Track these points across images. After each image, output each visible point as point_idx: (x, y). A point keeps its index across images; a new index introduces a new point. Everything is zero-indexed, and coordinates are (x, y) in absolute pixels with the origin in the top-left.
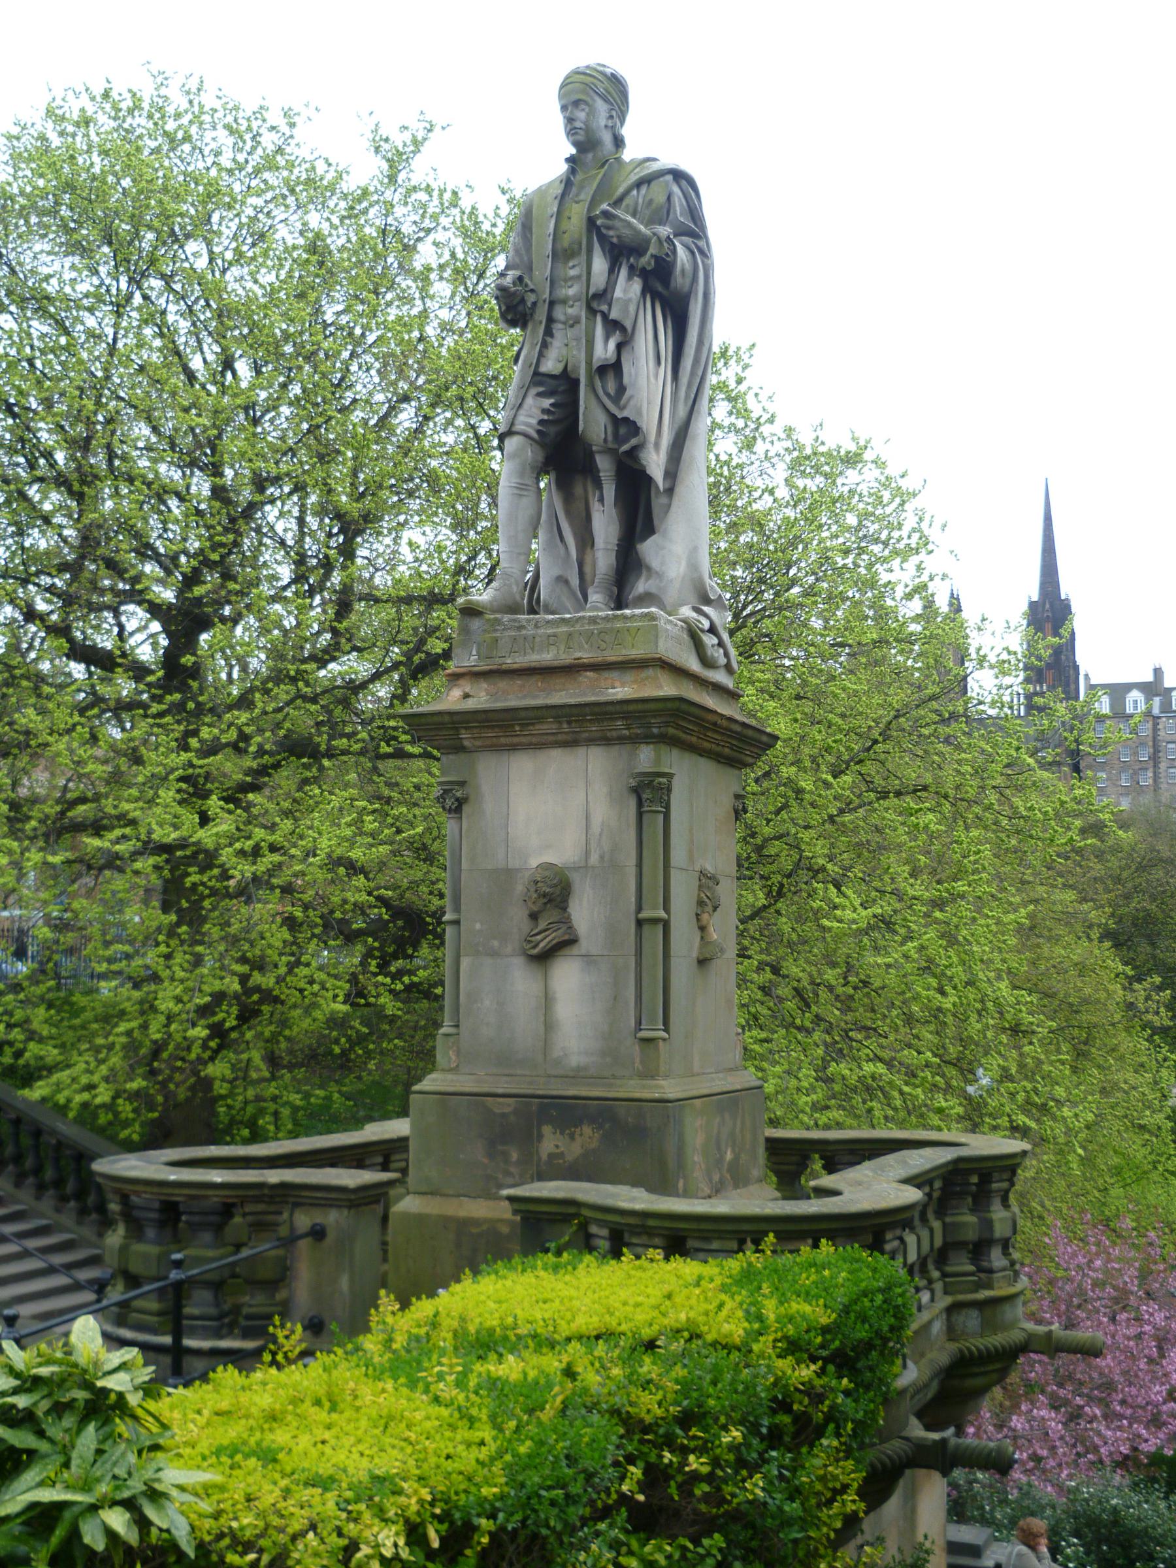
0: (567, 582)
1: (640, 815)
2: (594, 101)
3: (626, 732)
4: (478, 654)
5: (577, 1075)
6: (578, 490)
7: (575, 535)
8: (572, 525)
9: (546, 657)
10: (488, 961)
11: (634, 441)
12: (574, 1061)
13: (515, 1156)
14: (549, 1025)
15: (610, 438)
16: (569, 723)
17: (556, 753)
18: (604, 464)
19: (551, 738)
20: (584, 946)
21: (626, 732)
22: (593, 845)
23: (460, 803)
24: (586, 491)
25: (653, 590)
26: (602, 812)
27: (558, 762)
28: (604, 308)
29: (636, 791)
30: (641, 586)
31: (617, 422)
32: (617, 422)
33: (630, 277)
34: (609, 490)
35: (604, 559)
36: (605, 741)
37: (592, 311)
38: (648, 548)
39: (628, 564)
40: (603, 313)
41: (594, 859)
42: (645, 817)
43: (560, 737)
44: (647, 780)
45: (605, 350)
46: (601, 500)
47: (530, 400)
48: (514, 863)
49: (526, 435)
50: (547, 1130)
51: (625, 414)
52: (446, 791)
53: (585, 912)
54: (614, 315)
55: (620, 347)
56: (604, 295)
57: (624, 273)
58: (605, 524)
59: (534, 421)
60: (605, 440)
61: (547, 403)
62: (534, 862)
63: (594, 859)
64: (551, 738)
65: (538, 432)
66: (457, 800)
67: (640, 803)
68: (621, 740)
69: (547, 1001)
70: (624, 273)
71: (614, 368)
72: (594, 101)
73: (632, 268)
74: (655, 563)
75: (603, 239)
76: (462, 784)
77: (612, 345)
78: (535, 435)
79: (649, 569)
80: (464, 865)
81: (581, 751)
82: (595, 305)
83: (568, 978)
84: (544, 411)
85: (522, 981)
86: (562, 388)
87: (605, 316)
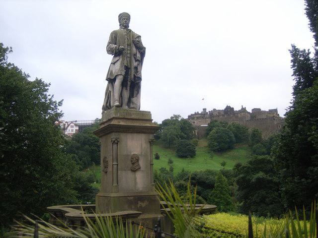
2: (125, 19)
5: (141, 192)
10: (124, 172)
12: (141, 189)
13: (133, 207)
14: (136, 183)
17: (135, 134)
20: (142, 169)
26: (144, 145)
29: (150, 142)
34: (128, 88)
38: (134, 99)
39: (129, 101)
41: (143, 154)
46: (127, 89)
48: (129, 154)
50: (139, 202)
53: (141, 163)
56: (135, 55)
58: (126, 94)
62: (132, 154)
63: (143, 154)
69: (135, 179)
72: (125, 19)
73: (139, 52)
74: (135, 102)
75: (135, 44)
79: (133, 103)
80: (118, 154)
83: (139, 175)
85: (130, 175)
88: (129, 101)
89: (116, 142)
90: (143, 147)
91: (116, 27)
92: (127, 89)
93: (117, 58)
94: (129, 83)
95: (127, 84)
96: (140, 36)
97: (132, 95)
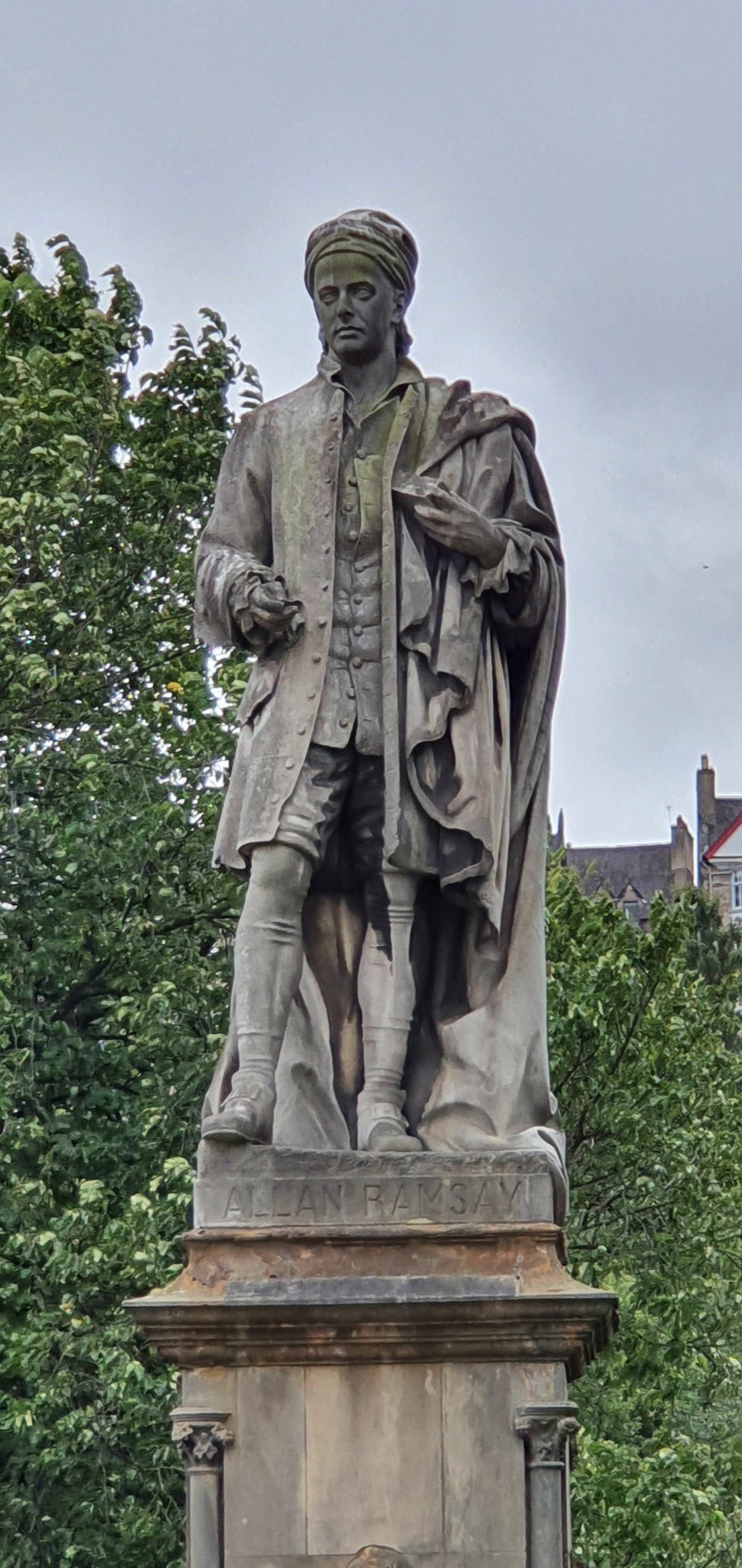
1: (528, 1470)
6: (326, 921)
9: (368, 1219)
11: (471, 870)
18: (398, 892)
25: (474, 1101)
28: (425, 648)
29: (526, 1439)
30: (449, 1089)
31: (434, 830)
32: (434, 830)
33: (464, 604)
34: (401, 935)
37: (402, 651)
38: (464, 1032)
39: (424, 1050)
40: (421, 657)
42: (535, 1476)
44: (545, 1419)
45: (425, 717)
46: (386, 948)
47: (303, 792)
49: (297, 849)
51: (458, 824)
52: (197, 1430)
54: (443, 666)
55: (453, 714)
57: (452, 593)
58: (386, 986)
59: (308, 826)
61: (325, 794)
66: (217, 1443)
70: (452, 593)
71: (442, 748)
73: (467, 587)
76: (223, 1418)
77: (436, 708)
79: (460, 1063)
82: (408, 643)
86: (344, 767)
87: (424, 662)
88: (424, 1050)
89: (202, 1448)
92: (386, 948)
94: (398, 892)
95: (384, 900)
96: (521, 425)
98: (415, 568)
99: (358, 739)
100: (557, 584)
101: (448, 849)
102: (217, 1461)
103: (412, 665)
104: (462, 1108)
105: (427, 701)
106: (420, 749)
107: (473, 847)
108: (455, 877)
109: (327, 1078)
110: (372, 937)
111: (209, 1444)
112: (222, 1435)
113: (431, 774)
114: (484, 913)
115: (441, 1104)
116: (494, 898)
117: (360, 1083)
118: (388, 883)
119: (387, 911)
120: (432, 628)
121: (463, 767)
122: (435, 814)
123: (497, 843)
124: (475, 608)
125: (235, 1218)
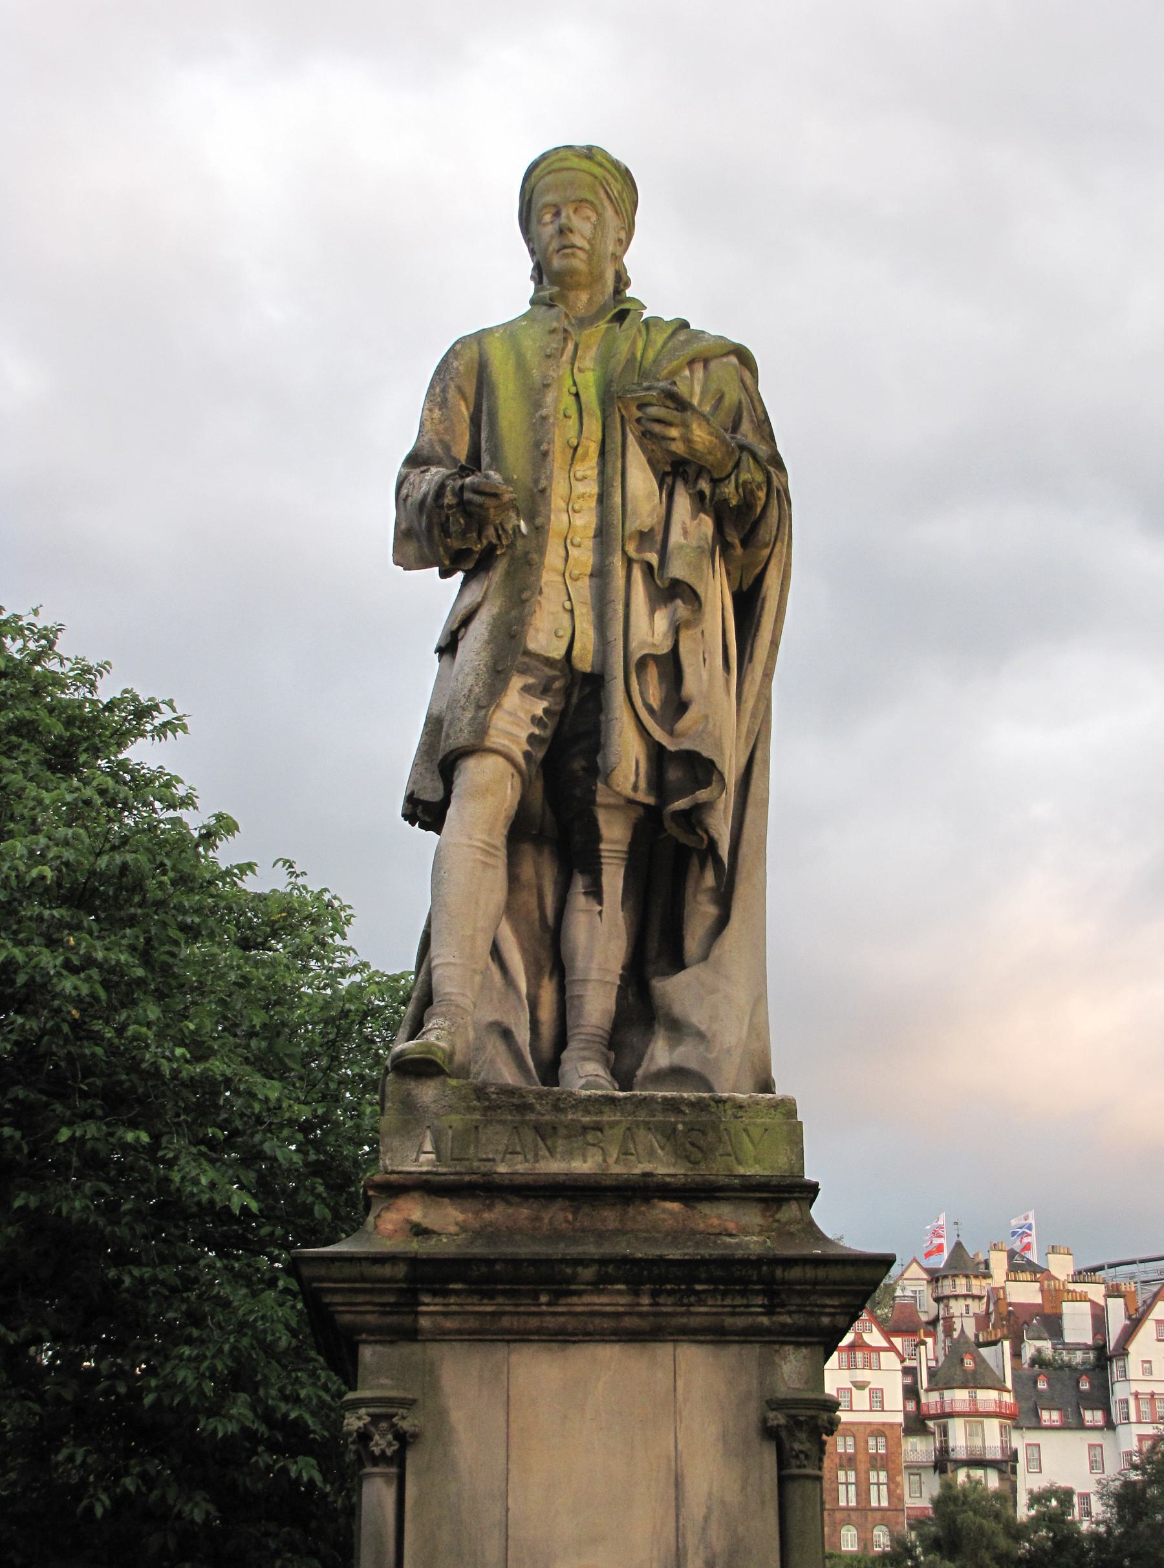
0: (506, 1034)
3: (765, 1320)
4: (437, 1151)
6: (527, 871)
7: (524, 951)
8: (516, 931)
15: (643, 784)
16: (655, 1294)
17: (610, 1353)
19: (607, 1324)
21: (765, 1320)
22: (691, 1541)
23: (404, 1440)
24: (539, 875)
25: (693, 1065)
27: (608, 1368)
28: (653, 558)
31: (658, 755)
34: (613, 879)
35: (597, 1004)
36: (716, 1335)
40: (648, 568)
43: (628, 1322)
45: (651, 629)
46: (595, 892)
51: (687, 745)
56: (657, 538)
60: (635, 788)
61: (539, 707)
64: (607, 1324)
65: (527, 755)
67: (781, 1464)
68: (748, 1335)
70: (683, 503)
73: (699, 499)
74: (697, 1017)
76: (408, 1404)
77: (662, 621)
78: (520, 759)
81: (663, 1351)
82: (632, 553)
84: (536, 721)
86: (557, 685)
90: (695, 1506)
91: (498, 286)
93: (475, 593)
95: (595, 836)
97: (659, 942)
98: (641, 481)
99: (576, 652)
100: (785, 518)
101: (674, 774)
102: (399, 1460)
103: (637, 574)
104: (677, 1074)
105: (652, 613)
106: (642, 663)
107: (701, 769)
108: (681, 804)
109: (523, 1036)
110: (579, 883)
111: (390, 1437)
112: (405, 1425)
113: (655, 693)
114: (713, 845)
115: (654, 1068)
116: (721, 829)
117: (561, 1041)
118: (602, 817)
119: (599, 850)
120: (659, 538)
121: (691, 685)
122: (659, 734)
123: (731, 767)
124: (707, 524)
125: (429, 1162)
